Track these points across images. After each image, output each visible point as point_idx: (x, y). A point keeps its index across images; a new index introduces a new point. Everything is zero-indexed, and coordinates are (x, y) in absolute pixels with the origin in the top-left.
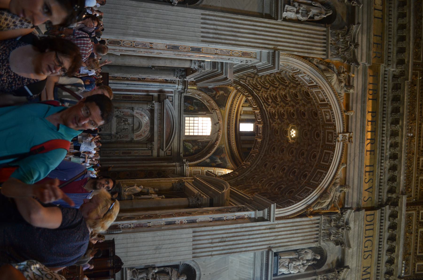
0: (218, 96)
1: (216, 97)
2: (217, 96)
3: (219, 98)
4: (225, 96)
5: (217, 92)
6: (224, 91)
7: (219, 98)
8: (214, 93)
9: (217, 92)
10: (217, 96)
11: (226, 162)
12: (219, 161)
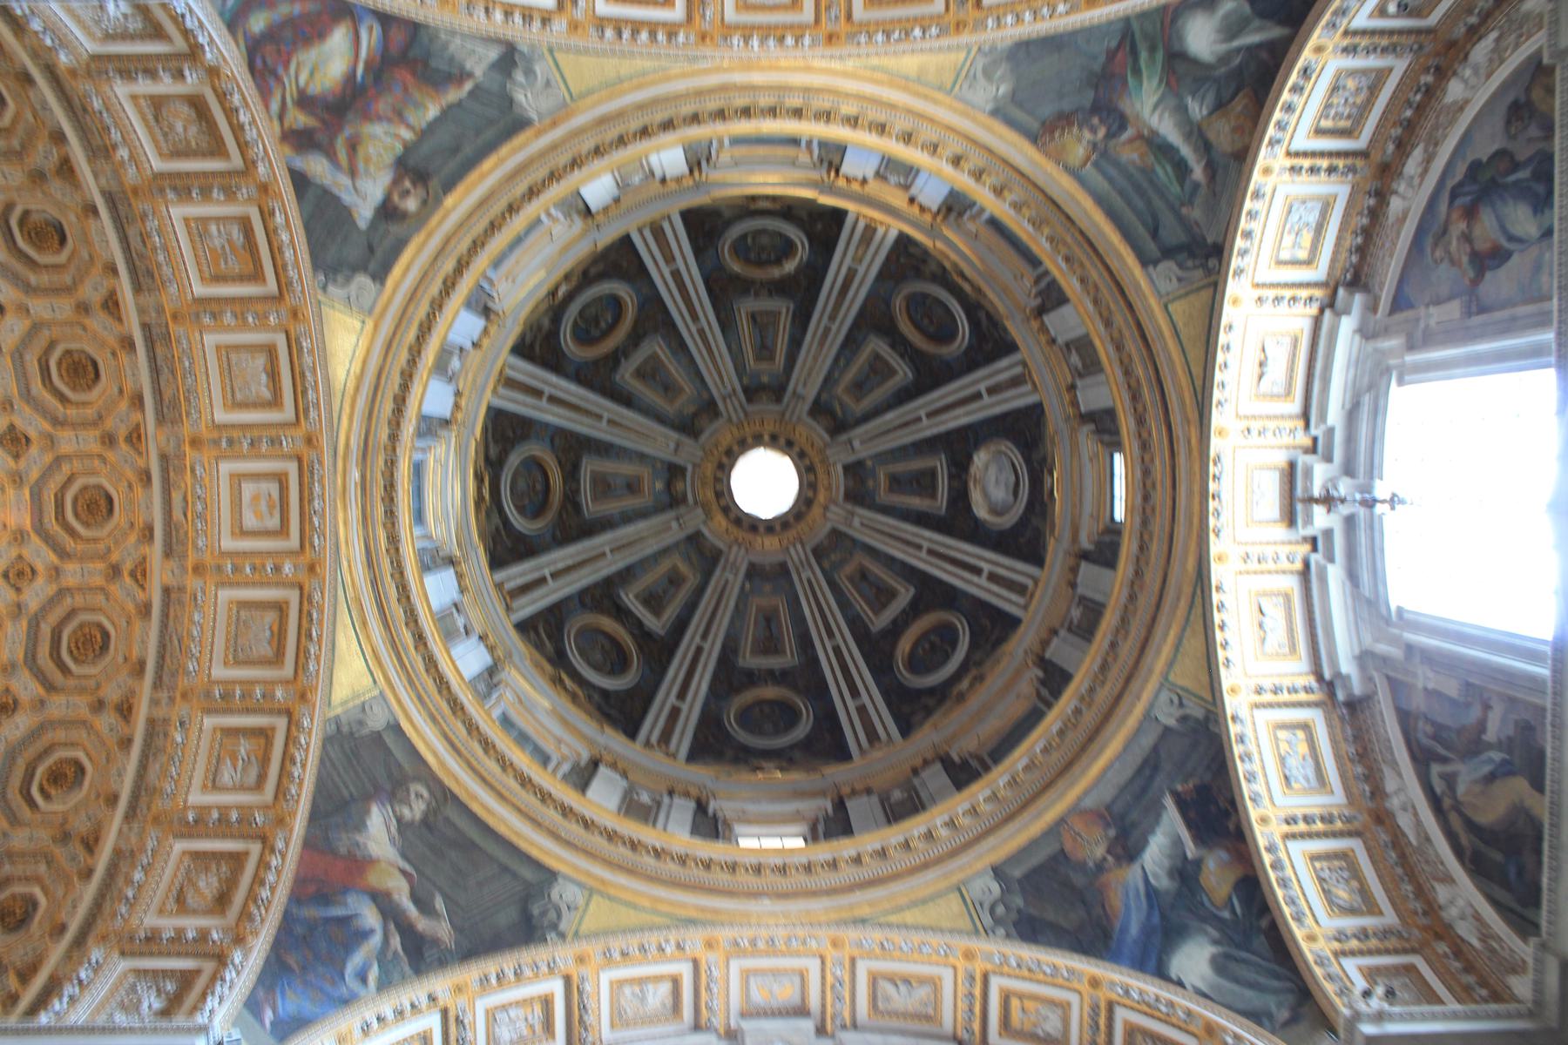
1: (422, 924)
3: (439, 904)
4: (426, 822)
5: (374, 879)
6: (367, 798)
7: (439, 904)
8: (370, 917)
9: (374, 879)
11: (1150, 766)
12: (1155, 853)
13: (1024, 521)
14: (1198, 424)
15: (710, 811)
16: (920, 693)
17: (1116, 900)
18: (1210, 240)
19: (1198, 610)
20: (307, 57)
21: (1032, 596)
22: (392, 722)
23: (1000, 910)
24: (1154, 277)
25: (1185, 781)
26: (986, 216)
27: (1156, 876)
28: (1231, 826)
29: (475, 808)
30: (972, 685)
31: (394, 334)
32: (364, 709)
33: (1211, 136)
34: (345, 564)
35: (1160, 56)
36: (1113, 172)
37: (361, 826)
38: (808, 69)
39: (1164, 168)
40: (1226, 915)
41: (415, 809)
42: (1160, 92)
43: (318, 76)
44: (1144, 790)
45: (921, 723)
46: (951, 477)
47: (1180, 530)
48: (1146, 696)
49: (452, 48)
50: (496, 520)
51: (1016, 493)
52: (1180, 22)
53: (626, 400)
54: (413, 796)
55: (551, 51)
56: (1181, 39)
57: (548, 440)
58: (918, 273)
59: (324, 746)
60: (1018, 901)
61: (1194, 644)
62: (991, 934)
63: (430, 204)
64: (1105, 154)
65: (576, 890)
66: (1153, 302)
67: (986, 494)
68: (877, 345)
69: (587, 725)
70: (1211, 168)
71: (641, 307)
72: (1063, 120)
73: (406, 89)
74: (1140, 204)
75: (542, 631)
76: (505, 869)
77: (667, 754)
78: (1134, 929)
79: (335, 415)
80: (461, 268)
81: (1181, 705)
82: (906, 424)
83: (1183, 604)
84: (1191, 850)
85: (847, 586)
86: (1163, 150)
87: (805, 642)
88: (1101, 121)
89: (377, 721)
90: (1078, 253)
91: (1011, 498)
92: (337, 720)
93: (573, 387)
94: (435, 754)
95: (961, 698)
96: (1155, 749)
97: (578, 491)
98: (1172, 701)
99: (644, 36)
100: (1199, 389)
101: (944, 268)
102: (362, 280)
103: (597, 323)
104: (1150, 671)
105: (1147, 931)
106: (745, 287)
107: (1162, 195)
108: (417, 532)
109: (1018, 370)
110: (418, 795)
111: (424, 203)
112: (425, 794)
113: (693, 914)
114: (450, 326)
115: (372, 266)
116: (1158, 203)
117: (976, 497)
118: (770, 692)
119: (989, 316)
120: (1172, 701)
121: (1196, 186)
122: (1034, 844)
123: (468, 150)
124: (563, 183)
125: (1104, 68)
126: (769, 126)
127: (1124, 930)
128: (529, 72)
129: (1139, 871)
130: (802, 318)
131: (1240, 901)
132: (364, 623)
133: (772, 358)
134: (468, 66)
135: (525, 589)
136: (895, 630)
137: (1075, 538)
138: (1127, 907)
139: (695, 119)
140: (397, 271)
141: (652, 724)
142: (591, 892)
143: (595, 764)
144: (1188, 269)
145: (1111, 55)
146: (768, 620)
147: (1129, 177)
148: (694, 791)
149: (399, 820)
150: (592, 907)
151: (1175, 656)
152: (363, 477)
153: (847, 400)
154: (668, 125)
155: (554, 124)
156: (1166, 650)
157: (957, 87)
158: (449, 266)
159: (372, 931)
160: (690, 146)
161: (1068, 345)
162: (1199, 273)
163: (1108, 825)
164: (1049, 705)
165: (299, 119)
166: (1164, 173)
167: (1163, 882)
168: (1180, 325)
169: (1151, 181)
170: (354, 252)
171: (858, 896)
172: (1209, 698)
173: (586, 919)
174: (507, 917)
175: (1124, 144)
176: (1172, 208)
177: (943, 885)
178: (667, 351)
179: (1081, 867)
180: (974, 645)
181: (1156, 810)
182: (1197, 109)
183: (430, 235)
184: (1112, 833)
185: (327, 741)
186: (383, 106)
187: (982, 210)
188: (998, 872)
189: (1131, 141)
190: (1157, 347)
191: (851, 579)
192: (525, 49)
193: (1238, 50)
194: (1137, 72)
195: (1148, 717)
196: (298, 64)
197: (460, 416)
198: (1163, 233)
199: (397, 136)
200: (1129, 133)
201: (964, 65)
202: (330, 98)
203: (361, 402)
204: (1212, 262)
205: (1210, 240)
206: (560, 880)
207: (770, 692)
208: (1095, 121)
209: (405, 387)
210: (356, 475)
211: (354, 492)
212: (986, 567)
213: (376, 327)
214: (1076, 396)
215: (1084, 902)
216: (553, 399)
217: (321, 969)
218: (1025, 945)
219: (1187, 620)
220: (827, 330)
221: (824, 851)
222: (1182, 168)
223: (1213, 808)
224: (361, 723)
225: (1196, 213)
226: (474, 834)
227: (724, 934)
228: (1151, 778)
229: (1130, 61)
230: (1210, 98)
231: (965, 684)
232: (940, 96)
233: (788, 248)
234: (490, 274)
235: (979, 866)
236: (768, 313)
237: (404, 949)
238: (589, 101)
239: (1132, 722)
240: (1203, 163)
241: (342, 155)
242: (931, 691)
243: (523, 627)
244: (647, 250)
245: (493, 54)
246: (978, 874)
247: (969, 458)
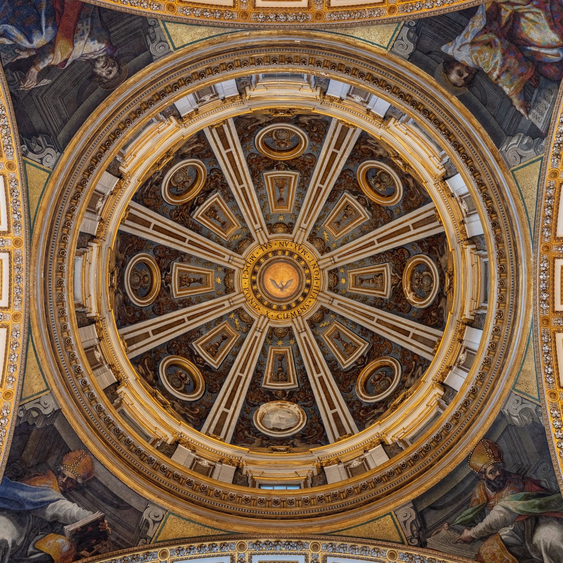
0: (47, 71)
1: (34, 71)
2: (41, 66)
4: (94, 75)
5: (62, 43)
6: (109, 43)
8: (39, 41)
9: (62, 43)
10: (41, 66)
13: (257, 433)
14: (320, 532)
15: (90, 244)
16: (156, 371)
17: (39, 483)
18: (428, 540)
19: (211, 532)
20: (543, 21)
21: (215, 438)
22: (154, 58)
23: (35, 414)
24: (407, 507)
25: (110, 525)
26: (441, 411)
27: (54, 507)
28: (83, 553)
29: (102, 105)
30: (161, 401)
31: (380, 66)
32: (161, 41)
33: (490, 541)
34: (248, 33)
35: (537, 511)
36: (468, 483)
37: (92, 37)
38: (528, 307)
39: (471, 513)
40: (31, 549)
41: (101, 70)
42: (514, 510)
43: (531, 24)
44: (104, 500)
45: (138, 371)
46: (284, 391)
47: (258, 522)
48: (161, 502)
49: (545, 102)
50: (263, 120)
51: (273, 429)
52: (556, 522)
53: (332, 199)
54: (110, 68)
55: (541, 158)
56: (547, 523)
57: (311, 152)
58: (406, 373)
59: (142, 17)
60: (39, 426)
61: (191, 531)
62: (21, 408)
63: (453, 88)
64: (478, 478)
65: (53, 162)
66: (392, 506)
67: (275, 411)
68: (363, 348)
69: (139, 172)
70: (471, 541)
71: (387, 208)
72: (498, 455)
73: (522, 75)
74: (449, 499)
75: (198, 145)
76: (65, 122)
77: (123, 220)
78: (22, 494)
79: (334, 30)
80: (414, 104)
81: (155, 522)
82: (315, 364)
83: (215, 523)
84: (69, 528)
85: (220, 327)
86: (481, 513)
87: (186, 303)
88: (497, 476)
89: (154, 49)
90: (419, 463)
91: (271, 427)
92: (156, 25)
93: (340, 167)
94: (135, 82)
95: (154, 395)
96: (130, 507)
97: (278, 168)
98: (156, 517)
99: (549, 212)
100: (340, 533)
101: (408, 388)
102: (412, 47)
103: (376, 182)
104: (174, 504)
105: (20, 502)
106: (399, 270)
107: (454, 512)
108: (261, 75)
109: (348, 431)
110: (110, 72)
111: (455, 85)
112: (111, 76)
113: (37, 231)
114: (379, 96)
115: (419, 53)
116: (450, 510)
117: (273, 405)
118: (157, 281)
119: (380, 414)
120: (156, 517)
121: (461, 532)
122: (74, 434)
123: (484, 110)
124: (464, 165)
125: (530, 479)
126: (494, 285)
127: (22, 489)
128: (529, 146)
129: (56, 497)
130: (380, 304)
131: (38, 558)
132: (211, 44)
133: (355, 285)
134: (534, 111)
135: (223, 137)
136: (193, 356)
137: (248, 462)
138: (35, 490)
139: (499, 240)
140: (415, 68)
141: (142, 211)
142: (50, 173)
143: (120, 176)
144: (411, 527)
145: (537, 483)
146: (200, 281)
147: (465, 493)
148: (102, 233)
149: (96, 60)
150: (43, 173)
151: (183, 519)
152: (296, 45)
153: (331, 328)
154: (495, 225)
155: (498, 161)
156: (187, 514)
157: (516, 393)
158: (417, 97)
159: (31, 42)
160: (483, 239)
161: (365, 459)
162: (409, 534)
163: (83, 479)
164: (153, 444)
165: (505, 14)
166: (468, 513)
167: (49, 512)
168: (378, 522)
169: (462, 506)
170: (427, 43)
171: (44, 330)
172: (158, 540)
173: (35, 168)
174: (37, 122)
175: (484, 490)
176: (447, 518)
177: (51, 381)
178: (360, 224)
179: (60, 462)
180: (183, 403)
181: (92, 508)
182: (505, 532)
183: (436, 87)
184: (80, 481)
185: (144, 19)
186: (512, 61)
187: (444, 409)
188: (58, 413)
189: (486, 494)
190: (365, 509)
191: (224, 330)
192: (543, 144)
193: (541, 556)
194: (527, 498)
195: (148, 502)
196: (539, 14)
197: (327, 100)
198: (433, 512)
199: (494, 69)
200: (491, 494)
201: (530, 397)
202: (519, 31)
203: (340, 45)
204: (416, 542)
205: (428, 540)
206: (58, 154)
207: (157, 281)
208: (498, 473)
209: (347, 71)
210: (297, 41)
211: (287, 40)
212: (230, 412)
213: (384, 55)
214: (334, 464)
215: (38, 464)
216: (334, 155)
217: (10, 10)
218: (13, 429)
219: (205, 526)
220: (372, 318)
221: (70, 310)
222: (471, 523)
223: (94, 541)
224: (152, 41)
225: (444, 532)
226: (87, 103)
227: (22, 250)
228: (112, 505)
229: (534, 493)
230: (512, 540)
231: (161, 397)
232: (512, 382)
233: (421, 295)
234: (412, 120)
235: (61, 402)
236: (382, 283)
237: (21, 59)
238: (511, 181)
239: (146, 494)
240: (473, 536)
241: (485, 37)
242: (157, 378)
243: (200, 135)
244: (421, 212)
245: (540, 126)
246: (56, 401)
247: (296, 402)
